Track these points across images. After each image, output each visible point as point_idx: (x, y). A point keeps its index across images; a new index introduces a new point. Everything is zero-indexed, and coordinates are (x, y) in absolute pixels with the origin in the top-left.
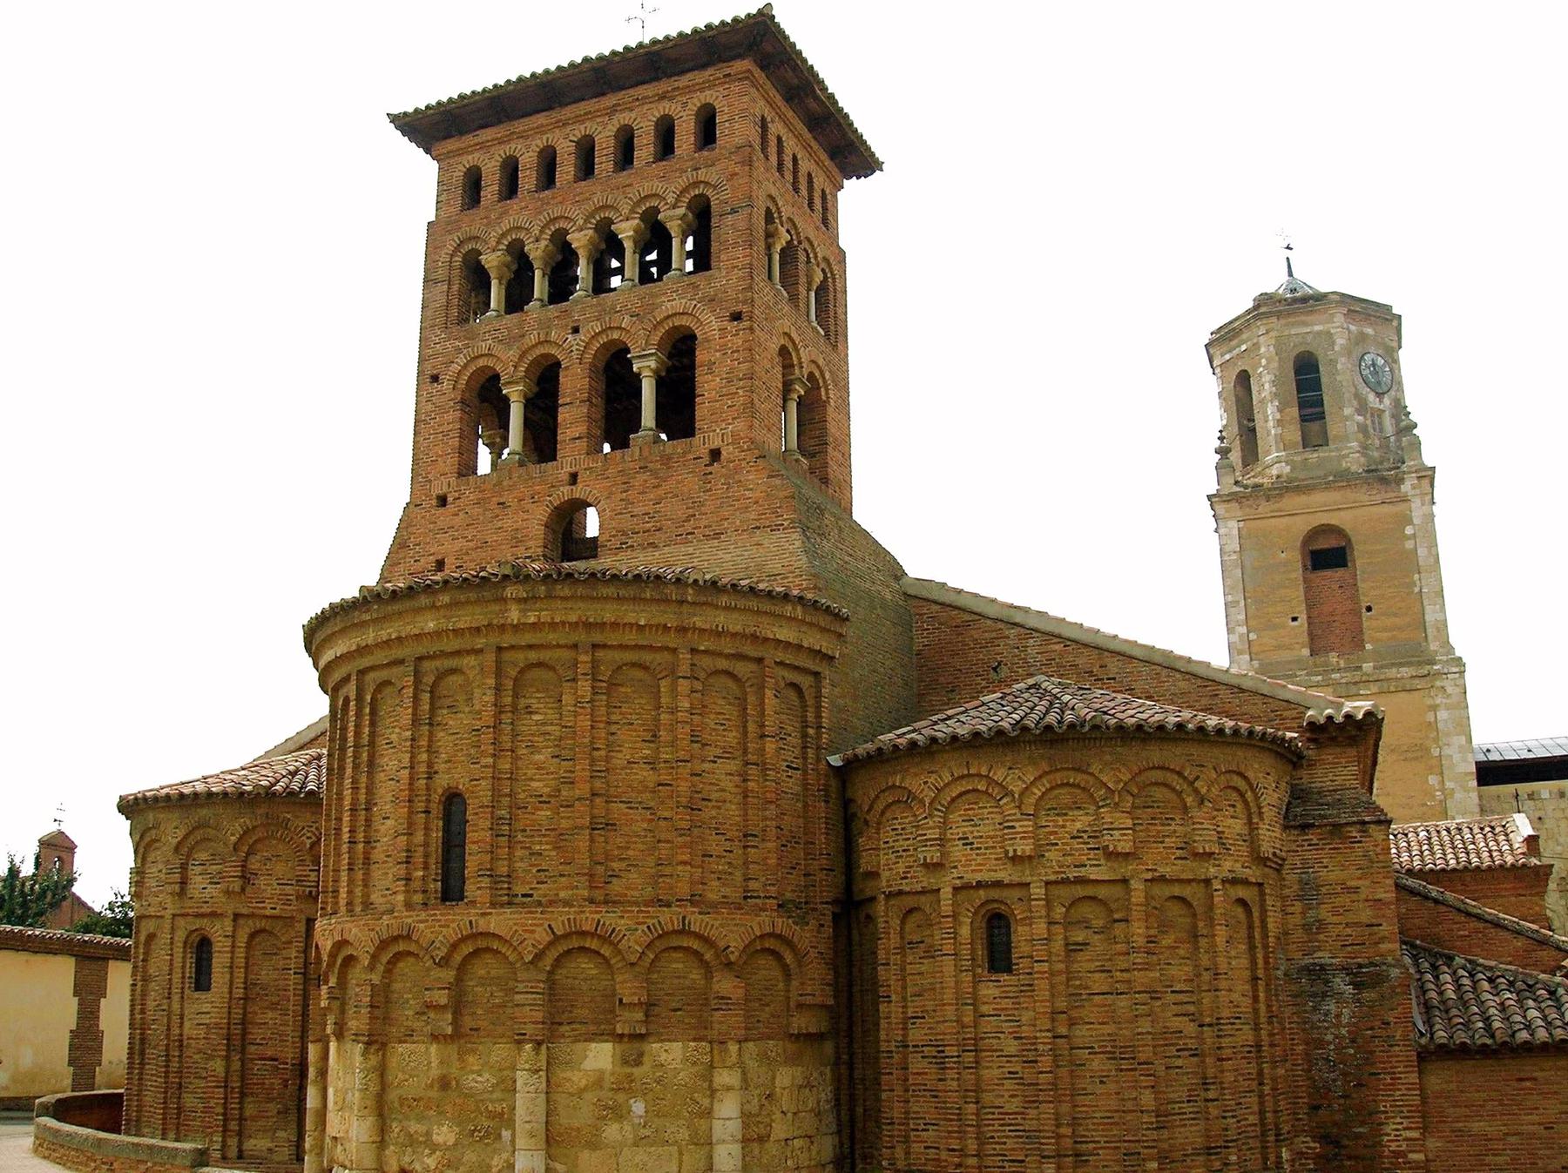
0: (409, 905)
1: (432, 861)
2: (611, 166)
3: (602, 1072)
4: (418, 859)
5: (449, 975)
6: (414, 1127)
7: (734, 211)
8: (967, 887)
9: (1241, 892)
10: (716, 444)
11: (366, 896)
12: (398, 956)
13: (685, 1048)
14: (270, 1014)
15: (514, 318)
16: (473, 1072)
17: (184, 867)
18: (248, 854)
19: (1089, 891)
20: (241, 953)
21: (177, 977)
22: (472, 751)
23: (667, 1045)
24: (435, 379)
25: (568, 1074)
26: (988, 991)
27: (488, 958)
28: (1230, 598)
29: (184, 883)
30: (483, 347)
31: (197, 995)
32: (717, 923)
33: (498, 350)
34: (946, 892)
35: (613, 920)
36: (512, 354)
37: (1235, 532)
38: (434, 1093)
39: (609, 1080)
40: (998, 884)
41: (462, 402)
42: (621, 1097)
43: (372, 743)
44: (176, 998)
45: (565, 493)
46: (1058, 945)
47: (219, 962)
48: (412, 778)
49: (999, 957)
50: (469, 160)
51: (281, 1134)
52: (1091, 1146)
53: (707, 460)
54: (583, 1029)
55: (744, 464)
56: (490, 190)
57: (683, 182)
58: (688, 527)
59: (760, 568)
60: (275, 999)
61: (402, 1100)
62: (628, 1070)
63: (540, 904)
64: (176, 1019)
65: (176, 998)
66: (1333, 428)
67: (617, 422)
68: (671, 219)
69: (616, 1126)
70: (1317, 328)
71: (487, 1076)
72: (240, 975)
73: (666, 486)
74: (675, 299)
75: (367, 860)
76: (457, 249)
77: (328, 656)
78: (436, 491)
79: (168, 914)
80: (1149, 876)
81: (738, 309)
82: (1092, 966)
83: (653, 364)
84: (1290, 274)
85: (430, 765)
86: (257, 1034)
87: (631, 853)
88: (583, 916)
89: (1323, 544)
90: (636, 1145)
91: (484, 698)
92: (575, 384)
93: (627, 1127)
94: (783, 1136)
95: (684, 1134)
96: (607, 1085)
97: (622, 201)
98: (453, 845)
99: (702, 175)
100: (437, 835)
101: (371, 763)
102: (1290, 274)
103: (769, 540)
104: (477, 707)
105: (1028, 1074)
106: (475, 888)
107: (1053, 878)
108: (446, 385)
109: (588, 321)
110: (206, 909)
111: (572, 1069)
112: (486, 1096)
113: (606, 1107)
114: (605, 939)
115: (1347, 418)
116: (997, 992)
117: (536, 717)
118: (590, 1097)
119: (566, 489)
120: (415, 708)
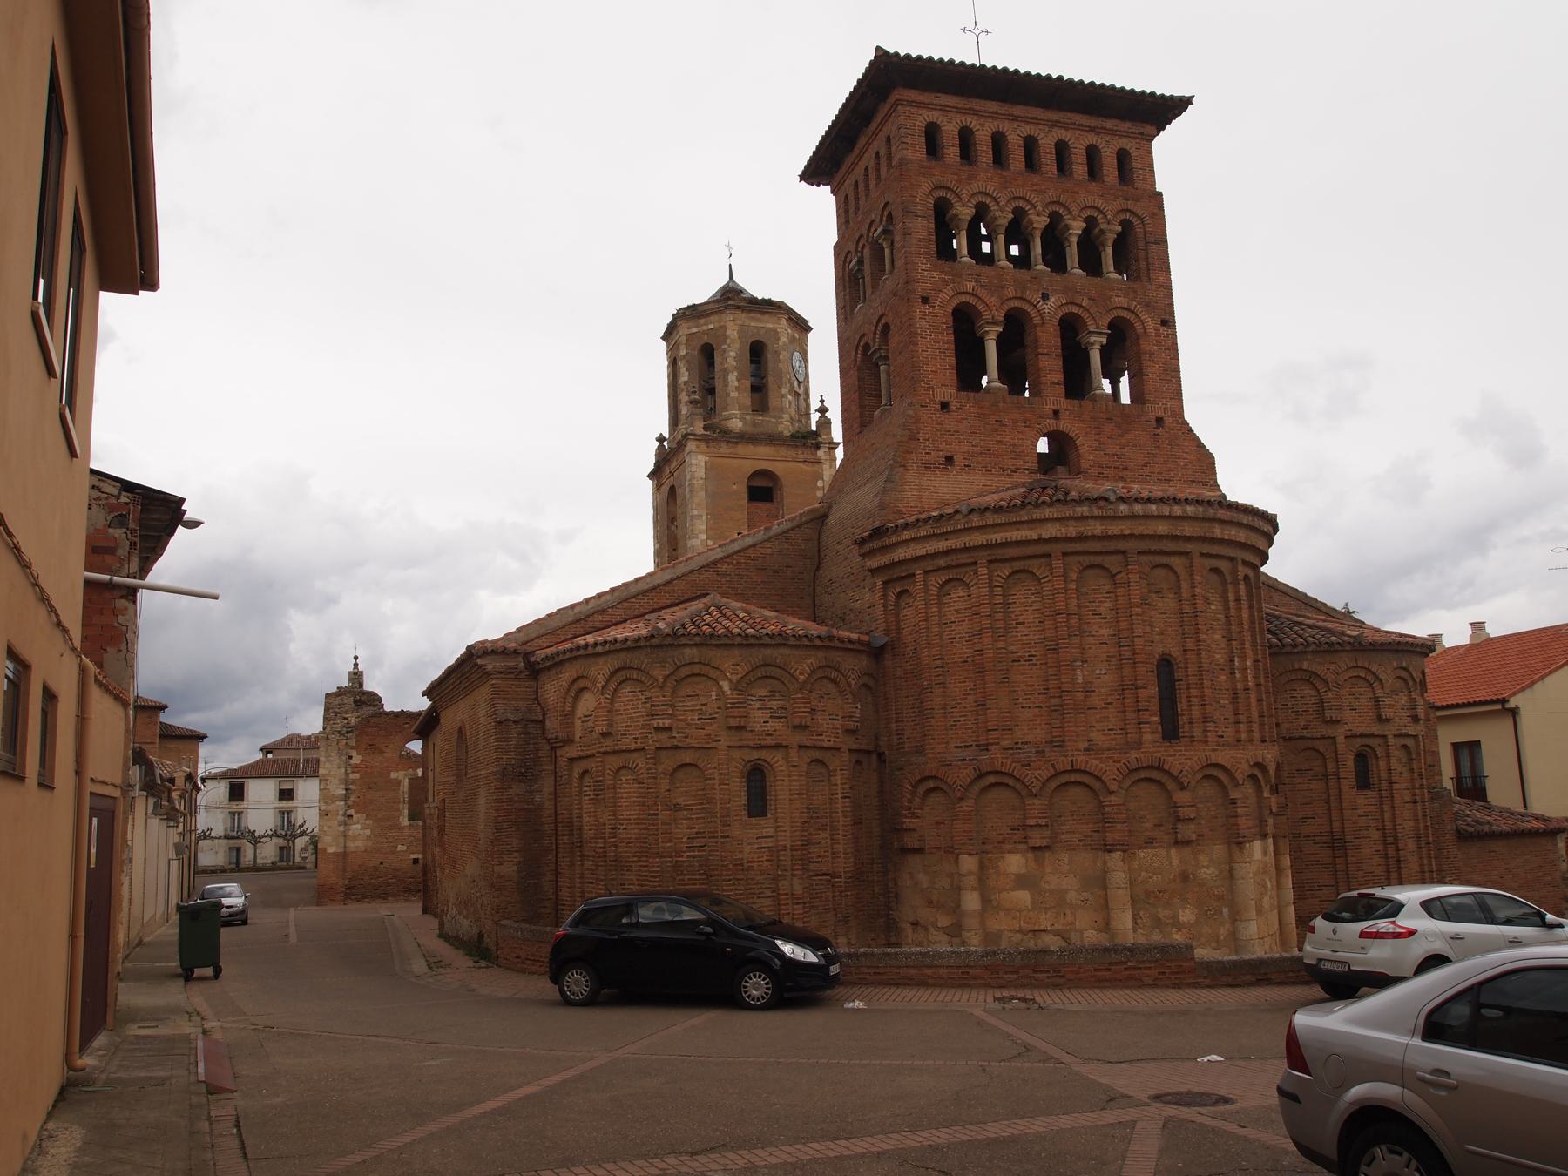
8: (1354, 736)
9: (1403, 741)
10: (1160, 414)
14: (823, 835)
30: (969, 286)
40: (1372, 735)
45: (1051, 424)
50: (933, 116)
53: (1154, 424)
58: (1146, 471)
66: (773, 402)
84: (731, 277)
102: (731, 277)
110: (769, 741)
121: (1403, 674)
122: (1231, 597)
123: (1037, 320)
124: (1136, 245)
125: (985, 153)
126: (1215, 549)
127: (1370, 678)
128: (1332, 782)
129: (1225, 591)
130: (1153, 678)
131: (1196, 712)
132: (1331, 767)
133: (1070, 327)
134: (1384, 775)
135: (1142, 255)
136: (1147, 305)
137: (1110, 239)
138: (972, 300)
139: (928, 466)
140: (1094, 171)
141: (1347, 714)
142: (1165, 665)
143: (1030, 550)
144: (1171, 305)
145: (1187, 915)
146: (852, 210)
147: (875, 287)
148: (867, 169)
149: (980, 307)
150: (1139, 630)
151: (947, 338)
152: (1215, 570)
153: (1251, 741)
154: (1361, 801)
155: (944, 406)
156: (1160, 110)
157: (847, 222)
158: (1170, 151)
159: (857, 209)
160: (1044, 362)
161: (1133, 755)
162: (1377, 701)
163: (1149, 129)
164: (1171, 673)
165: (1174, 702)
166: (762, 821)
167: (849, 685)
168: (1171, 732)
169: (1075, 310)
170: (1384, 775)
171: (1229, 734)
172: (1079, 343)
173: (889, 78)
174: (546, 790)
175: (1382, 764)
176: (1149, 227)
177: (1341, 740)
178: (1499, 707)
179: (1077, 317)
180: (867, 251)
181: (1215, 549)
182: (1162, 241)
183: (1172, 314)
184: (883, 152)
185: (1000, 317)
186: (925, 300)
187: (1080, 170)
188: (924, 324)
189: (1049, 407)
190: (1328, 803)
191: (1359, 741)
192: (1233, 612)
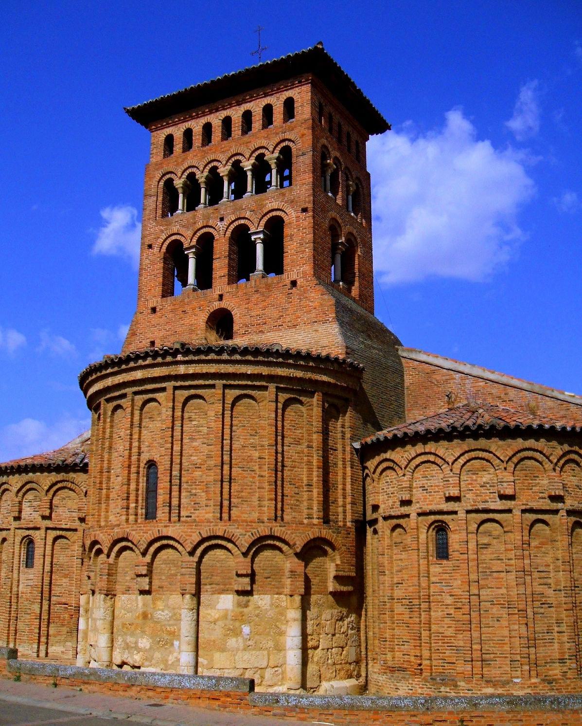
0: (127, 520)
1: (140, 498)
2: (240, 132)
3: (227, 610)
4: (132, 497)
5: (148, 558)
6: (130, 639)
7: (303, 154)
10: (294, 278)
11: (107, 517)
12: (125, 549)
13: (272, 598)
14: (64, 580)
15: (191, 214)
16: (159, 610)
17: (20, 503)
18: (54, 495)
19: (491, 516)
20: (49, 548)
21: (16, 561)
22: (161, 441)
23: (262, 596)
24: (150, 246)
25: (209, 611)
26: (435, 569)
27: (170, 550)
29: (20, 512)
31: (26, 570)
32: (289, 532)
33: (182, 231)
34: (413, 516)
35: (233, 530)
36: (189, 233)
38: (140, 621)
39: (230, 614)
40: (441, 513)
41: (164, 258)
42: (237, 624)
43: (111, 437)
44: (16, 572)
45: (217, 305)
46: (472, 545)
47: (38, 552)
48: (130, 456)
49: (443, 552)
51: (69, 644)
52: (492, 656)
53: (289, 286)
54: (218, 587)
55: (309, 288)
56: (178, 147)
57: (277, 140)
58: (280, 322)
59: (317, 342)
60: (67, 572)
61: (124, 625)
62: (242, 610)
63: (195, 521)
64: (15, 583)
65: (16, 572)
67: (242, 268)
68: (271, 159)
69: (234, 640)
71: (166, 612)
72: (48, 559)
73: (268, 301)
74: (272, 200)
75: (108, 497)
76: (161, 178)
77: (92, 391)
78: (151, 305)
79: (12, 528)
80: (524, 507)
81: (305, 206)
82: (493, 556)
83: (261, 236)
85: (139, 448)
86: (56, 590)
87: (243, 494)
88: (217, 528)
90: (245, 649)
91: (166, 413)
92: (221, 247)
93: (240, 640)
94: (326, 647)
95: (271, 644)
96: (229, 617)
97: (245, 149)
98: (151, 491)
99: (287, 135)
100: (143, 485)
101: (110, 448)
103: (321, 328)
104: (164, 417)
105: (458, 615)
106: (162, 513)
107: (470, 508)
108: (156, 250)
109: (229, 214)
110: (31, 526)
111: (211, 608)
112: (166, 623)
113: (229, 629)
114: (229, 540)
116: (440, 570)
117: (194, 423)
118: (220, 623)
120: (132, 419)
127: (439, 461)
145: (144, 643)
155: (154, 310)
191: (432, 518)
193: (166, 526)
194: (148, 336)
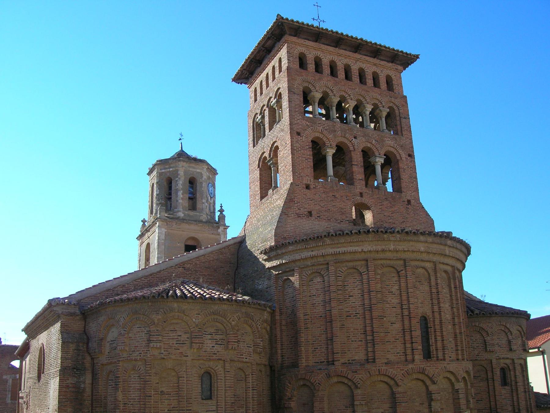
10: (409, 198)
28: (159, 255)
37: (164, 233)
66: (199, 206)
70: (198, 171)
89: (190, 243)
110: (215, 357)
115: (203, 203)
119: (359, 198)
121: (520, 329)
122: (453, 286)
123: (351, 148)
124: (396, 120)
125: (327, 70)
126: (446, 260)
127: (507, 331)
128: (490, 382)
129: (450, 282)
130: (418, 325)
131: (439, 344)
132: (490, 374)
133: (366, 154)
134: (513, 378)
135: (398, 123)
136: (402, 146)
137: (384, 114)
138: (321, 136)
139: (299, 216)
140: (376, 84)
141: (496, 348)
142: (424, 320)
143: (358, 256)
144: (412, 147)
146: (258, 94)
147: (271, 128)
148: (268, 74)
149: (325, 139)
150: (412, 300)
151: (309, 153)
152: (446, 272)
153: (463, 359)
154: (503, 392)
156: (405, 60)
157: (256, 100)
158: (410, 80)
159: (261, 93)
160: (355, 169)
161: (410, 366)
162: (509, 342)
163: (400, 67)
164: (426, 324)
165: (428, 340)
166: (209, 402)
167: (257, 328)
168: (427, 355)
169: (369, 145)
170: (513, 378)
171: (454, 356)
172: (370, 162)
173: (282, 30)
174: (87, 382)
175: (512, 373)
176: (401, 111)
177: (494, 361)
178: (536, 350)
179: (370, 149)
180: (267, 113)
181: (446, 260)
182: (407, 118)
183: (413, 151)
184: (277, 65)
185: (334, 145)
186: (299, 134)
187: (370, 82)
188: (298, 145)
189: (358, 191)
190: (489, 393)
192: (454, 294)
193: (448, 364)
194: (306, 206)
